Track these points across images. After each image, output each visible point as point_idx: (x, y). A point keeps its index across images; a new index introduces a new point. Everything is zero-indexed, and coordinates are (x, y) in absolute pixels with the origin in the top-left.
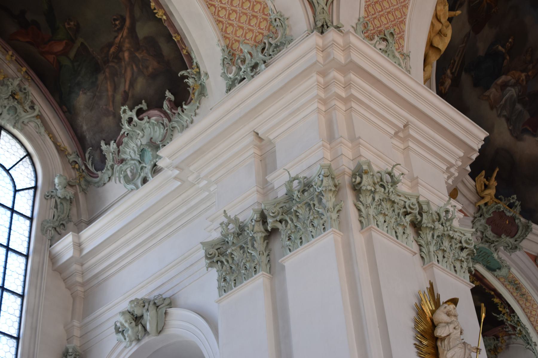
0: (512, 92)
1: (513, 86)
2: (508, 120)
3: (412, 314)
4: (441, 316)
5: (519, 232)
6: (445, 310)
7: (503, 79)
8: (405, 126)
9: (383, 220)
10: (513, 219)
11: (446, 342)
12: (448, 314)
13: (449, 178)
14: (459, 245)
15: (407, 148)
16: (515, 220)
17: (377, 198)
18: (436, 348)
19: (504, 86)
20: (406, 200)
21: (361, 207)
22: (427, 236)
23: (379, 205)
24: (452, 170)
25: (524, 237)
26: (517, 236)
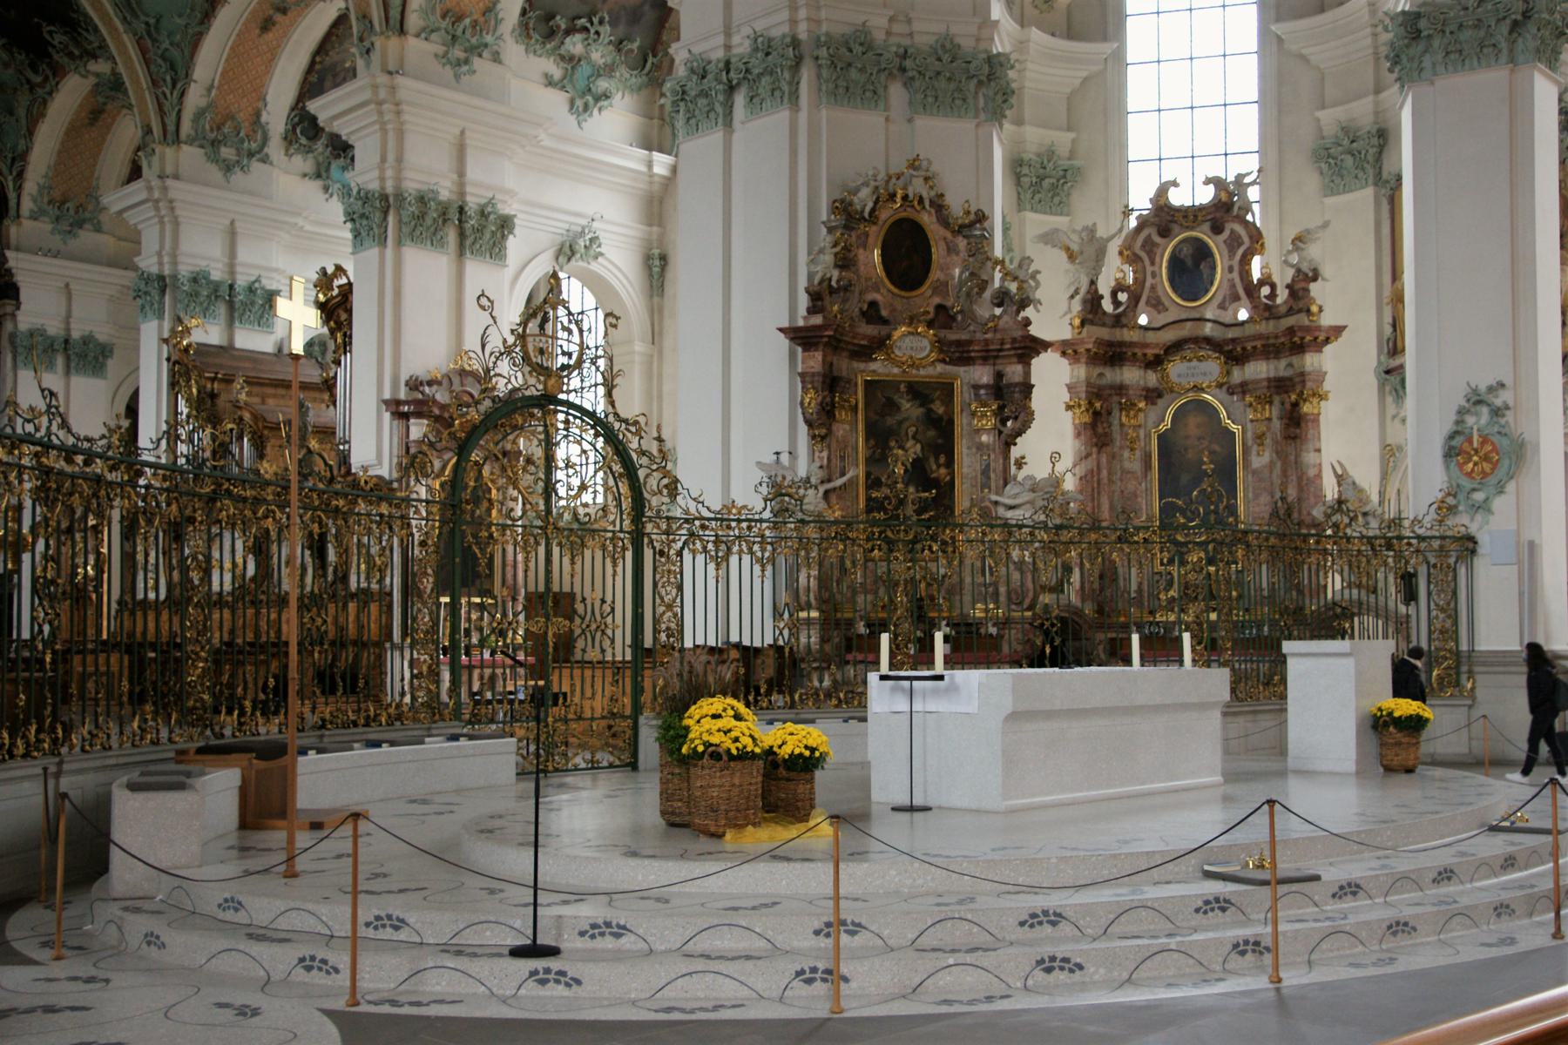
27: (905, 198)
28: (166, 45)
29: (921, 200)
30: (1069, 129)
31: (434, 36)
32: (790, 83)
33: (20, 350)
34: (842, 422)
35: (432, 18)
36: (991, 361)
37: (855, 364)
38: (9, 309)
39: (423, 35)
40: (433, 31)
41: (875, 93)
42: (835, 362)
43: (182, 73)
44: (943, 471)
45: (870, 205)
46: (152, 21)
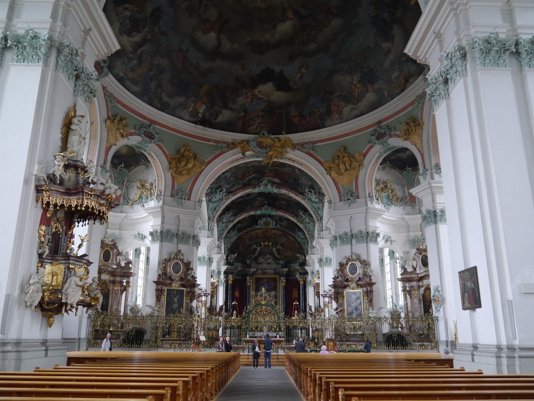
0: (128, 13)
1: (130, 11)
2: (121, 24)
3: (64, 116)
4: (75, 120)
5: (102, 75)
6: (79, 119)
7: (127, 5)
8: (90, 29)
9: (66, 70)
10: (103, 67)
11: (74, 132)
12: (79, 121)
13: (96, 58)
14: (91, 90)
15: (86, 38)
16: (103, 68)
17: (67, 59)
18: (68, 132)
19: (126, 9)
20: (78, 64)
21: (59, 60)
22: (80, 83)
23: (67, 63)
24: (100, 55)
25: (103, 77)
26: (101, 75)
28: (310, 232)
30: (421, 231)
34: (341, 300)
37: (344, 289)
38: (307, 276)
44: (360, 307)
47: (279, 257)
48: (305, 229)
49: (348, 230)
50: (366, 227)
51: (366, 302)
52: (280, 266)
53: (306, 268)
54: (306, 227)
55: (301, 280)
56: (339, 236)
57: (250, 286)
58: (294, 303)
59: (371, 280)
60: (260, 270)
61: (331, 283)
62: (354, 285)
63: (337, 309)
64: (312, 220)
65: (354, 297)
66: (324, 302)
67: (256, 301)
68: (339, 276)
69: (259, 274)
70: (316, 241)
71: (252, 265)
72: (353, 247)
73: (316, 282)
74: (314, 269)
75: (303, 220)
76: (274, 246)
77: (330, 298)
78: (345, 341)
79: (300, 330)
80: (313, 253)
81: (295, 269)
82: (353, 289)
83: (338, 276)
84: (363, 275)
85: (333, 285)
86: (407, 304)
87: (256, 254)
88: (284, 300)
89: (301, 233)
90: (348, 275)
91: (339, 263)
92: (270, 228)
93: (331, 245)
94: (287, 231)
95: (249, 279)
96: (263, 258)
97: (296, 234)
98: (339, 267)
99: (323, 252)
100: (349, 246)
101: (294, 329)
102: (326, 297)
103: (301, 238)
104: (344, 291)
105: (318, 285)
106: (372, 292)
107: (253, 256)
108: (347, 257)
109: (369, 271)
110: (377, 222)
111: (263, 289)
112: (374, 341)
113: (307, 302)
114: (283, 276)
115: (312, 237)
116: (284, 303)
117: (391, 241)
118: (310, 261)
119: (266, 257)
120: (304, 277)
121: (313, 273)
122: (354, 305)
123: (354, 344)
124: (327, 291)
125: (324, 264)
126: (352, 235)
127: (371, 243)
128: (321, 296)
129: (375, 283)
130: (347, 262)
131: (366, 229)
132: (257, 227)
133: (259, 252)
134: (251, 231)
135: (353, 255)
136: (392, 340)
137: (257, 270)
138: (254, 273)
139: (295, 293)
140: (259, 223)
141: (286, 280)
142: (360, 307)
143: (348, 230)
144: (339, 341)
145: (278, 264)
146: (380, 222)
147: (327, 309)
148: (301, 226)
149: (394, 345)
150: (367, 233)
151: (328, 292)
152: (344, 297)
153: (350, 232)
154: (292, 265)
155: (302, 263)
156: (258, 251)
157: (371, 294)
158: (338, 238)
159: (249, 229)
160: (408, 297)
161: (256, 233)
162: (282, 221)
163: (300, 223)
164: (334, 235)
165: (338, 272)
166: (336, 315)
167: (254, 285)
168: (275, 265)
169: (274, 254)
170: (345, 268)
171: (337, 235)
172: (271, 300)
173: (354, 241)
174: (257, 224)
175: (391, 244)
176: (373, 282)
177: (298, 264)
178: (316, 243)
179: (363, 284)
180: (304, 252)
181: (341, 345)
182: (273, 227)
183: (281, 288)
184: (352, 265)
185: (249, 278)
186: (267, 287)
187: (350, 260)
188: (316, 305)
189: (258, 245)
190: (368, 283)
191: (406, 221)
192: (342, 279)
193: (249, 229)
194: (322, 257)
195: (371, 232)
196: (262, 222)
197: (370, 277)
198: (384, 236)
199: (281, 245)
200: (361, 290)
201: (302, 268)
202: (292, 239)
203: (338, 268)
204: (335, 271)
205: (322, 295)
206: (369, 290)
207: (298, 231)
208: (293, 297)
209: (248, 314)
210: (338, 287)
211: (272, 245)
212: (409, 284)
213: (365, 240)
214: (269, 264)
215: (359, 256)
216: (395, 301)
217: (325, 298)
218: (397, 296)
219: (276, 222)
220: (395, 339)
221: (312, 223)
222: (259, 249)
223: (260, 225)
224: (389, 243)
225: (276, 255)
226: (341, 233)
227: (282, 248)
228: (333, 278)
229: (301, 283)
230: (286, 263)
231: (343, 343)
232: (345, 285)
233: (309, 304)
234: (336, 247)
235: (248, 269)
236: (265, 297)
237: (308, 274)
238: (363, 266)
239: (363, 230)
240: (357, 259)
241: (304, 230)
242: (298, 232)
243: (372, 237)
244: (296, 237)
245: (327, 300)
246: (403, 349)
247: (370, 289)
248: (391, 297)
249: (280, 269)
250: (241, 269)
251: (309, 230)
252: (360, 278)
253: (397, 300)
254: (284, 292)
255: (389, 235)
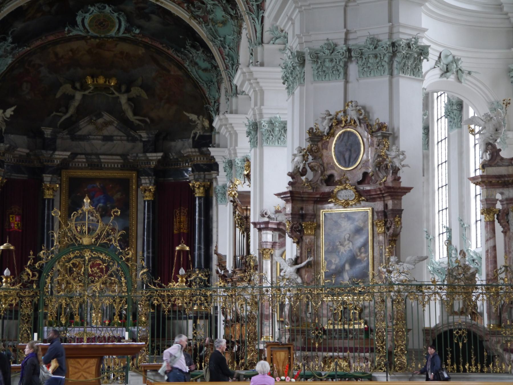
27: (346, 122)
28: (227, 49)
29: (355, 122)
31: (277, 41)
32: (300, 73)
33: (219, 195)
34: (310, 235)
35: (276, 33)
36: (383, 199)
37: (319, 206)
38: (214, 176)
39: (272, 42)
40: (277, 38)
41: (338, 70)
42: (304, 207)
43: (236, 61)
45: (327, 128)
46: (222, 39)
47: (137, 122)
48: (212, 41)
49: (338, 37)
50: (391, 28)
51: (379, 242)
52: (140, 145)
53: (213, 151)
54: (214, 35)
55: (197, 184)
56: (310, 54)
57: (53, 200)
58: (177, 248)
59: (397, 179)
60: (83, 156)
61: (284, 186)
62: (349, 194)
63: (299, 261)
64: (233, 13)
65: (347, 227)
66: (261, 243)
67: (65, 235)
68: (308, 169)
69: (81, 168)
70: (244, 73)
71: (59, 141)
72: (350, 86)
73: (240, 188)
74: (235, 154)
75: (209, 12)
76: (123, 88)
77: (277, 234)
78: (319, 350)
79: (191, 322)
80: (234, 108)
81: (181, 156)
82: (346, 205)
83: (304, 168)
84: (376, 166)
85: (291, 192)
86: (494, 248)
87: (72, 110)
88: (148, 241)
89: (200, 52)
90: (333, 167)
91: (309, 133)
92: (112, 37)
93: (285, 79)
94: (160, 46)
95: (50, 182)
96: (90, 122)
97: (185, 55)
98: (309, 144)
99: (262, 104)
100: (341, 84)
101: (175, 318)
102: (267, 228)
103: (199, 68)
104: (318, 210)
105: (245, 197)
106: (398, 212)
107: (61, 117)
108: (333, 113)
109: (393, 154)
110: (422, 14)
111: (87, 201)
112: (401, 350)
113: (214, 244)
114: (148, 175)
115: (233, 65)
116: (148, 248)
117: (459, 71)
118: (223, 131)
119: (100, 121)
120: (207, 177)
121: (231, 164)
122: (347, 248)
123: (345, 359)
124: (269, 213)
125: (264, 138)
126: (349, 50)
127: (401, 74)
128: (252, 226)
129: (409, 189)
130: (331, 128)
131: (391, 34)
132: (74, 33)
133: (79, 105)
134: (55, 43)
135: (349, 109)
136: (452, 347)
137: (74, 155)
138: (65, 165)
139: (180, 222)
140: (79, 19)
141: (156, 184)
142: (363, 255)
143: (338, 37)
144: (303, 349)
145: (134, 140)
146: (431, 14)
147: (269, 262)
148: (202, 31)
149: (456, 360)
150: (393, 44)
151: (273, 216)
152: (318, 226)
153: (343, 42)
154: (173, 144)
155: (200, 136)
156: (76, 103)
157: (397, 220)
158: (308, 58)
159: (51, 38)
160: (499, 228)
161: (71, 50)
162: (149, 19)
163: (199, 23)
164: (298, 49)
165: (303, 156)
166: (295, 276)
167: (63, 197)
168: (125, 142)
169: (123, 112)
170: (326, 146)
171: (306, 51)
172: (108, 235)
173: (353, 68)
174: (74, 24)
175: (459, 80)
176: (403, 185)
177: (191, 140)
178: (242, 78)
179: (375, 190)
180: (207, 108)
181: (307, 359)
182: (121, 34)
183: (140, 207)
184: (346, 138)
185: (49, 179)
186: (101, 205)
187: (339, 122)
188: (237, 254)
189: (78, 85)
190: (389, 188)
191: (506, 14)
192: (315, 176)
193: (51, 38)
194: (258, 117)
195: (403, 43)
196: (88, 18)
197: (396, 170)
198: (440, 57)
199: (141, 87)
200: (369, 210)
201: (202, 153)
202: (174, 71)
203: (306, 145)
204: (296, 152)
205: (255, 224)
206: (390, 207)
207: (193, 46)
208: (175, 232)
209: (40, 273)
210: (303, 201)
211: (118, 88)
212: (502, 194)
213: (386, 66)
214: (108, 139)
215: (367, 113)
216: (456, 242)
217: (264, 232)
218: (464, 227)
219: (128, 21)
220: (461, 345)
221: (231, 22)
222: (78, 96)
223: (81, 27)
224: (452, 78)
225: (130, 115)
226: (317, 46)
227: (144, 95)
228: (290, 175)
229: (199, 193)
230: (157, 136)
231: (314, 354)
232: (323, 194)
233: (220, 251)
234: (301, 84)
235: (46, 154)
236: (92, 225)
237: (217, 170)
238: (375, 140)
239: (381, 37)
240: (359, 119)
241: (210, 44)
242: (193, 51)
243: (406, 57)
244: (187, 64)
245: (268, 236)
246: (482, 371)
247: (394, 204)
248: (445, 230)
249: (140, 155)
250: (28, 151)
251: (223, 44)
252: (365, 174)
253: (464, 237)
254: (148, 218)
255: (454, 53)
